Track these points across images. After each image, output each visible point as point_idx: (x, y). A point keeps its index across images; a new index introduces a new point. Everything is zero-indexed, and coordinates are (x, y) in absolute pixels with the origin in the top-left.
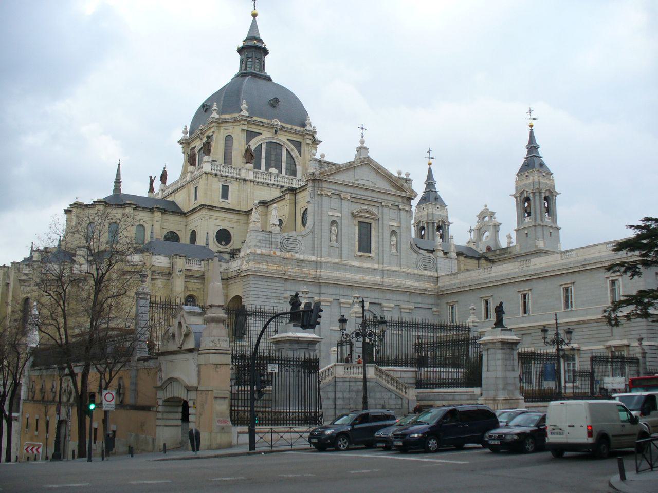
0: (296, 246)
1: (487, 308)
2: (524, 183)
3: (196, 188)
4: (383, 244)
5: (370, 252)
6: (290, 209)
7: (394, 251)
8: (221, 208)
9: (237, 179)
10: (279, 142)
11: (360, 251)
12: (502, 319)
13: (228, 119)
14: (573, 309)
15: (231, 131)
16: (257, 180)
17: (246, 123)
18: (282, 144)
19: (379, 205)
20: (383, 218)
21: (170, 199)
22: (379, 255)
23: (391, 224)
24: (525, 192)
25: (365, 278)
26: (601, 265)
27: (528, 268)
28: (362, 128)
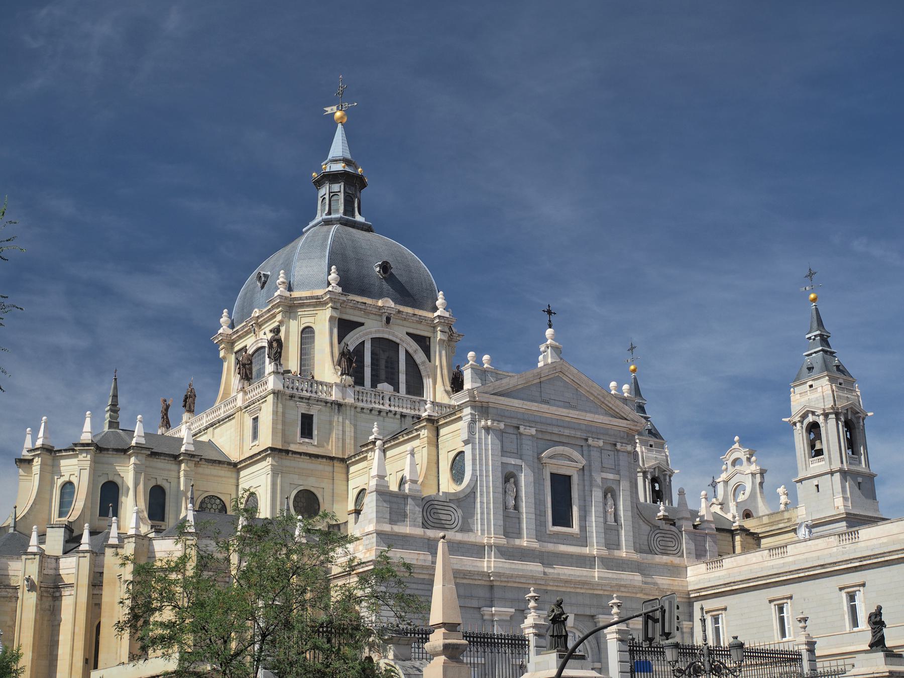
0: (449, 518)
2: (806, 398)
3: (256, 419)
8: (300, 454)
9: (326, 403)
10: (391, 338)
12: (882, 638)
13: (306, 298)
15: (311, 319)
16: (360, 404)
18: (398, 341)
19: (583, 443)
21: (204, 438)
24: (810, 415)
27: (853, 546)
28: (549, 312)
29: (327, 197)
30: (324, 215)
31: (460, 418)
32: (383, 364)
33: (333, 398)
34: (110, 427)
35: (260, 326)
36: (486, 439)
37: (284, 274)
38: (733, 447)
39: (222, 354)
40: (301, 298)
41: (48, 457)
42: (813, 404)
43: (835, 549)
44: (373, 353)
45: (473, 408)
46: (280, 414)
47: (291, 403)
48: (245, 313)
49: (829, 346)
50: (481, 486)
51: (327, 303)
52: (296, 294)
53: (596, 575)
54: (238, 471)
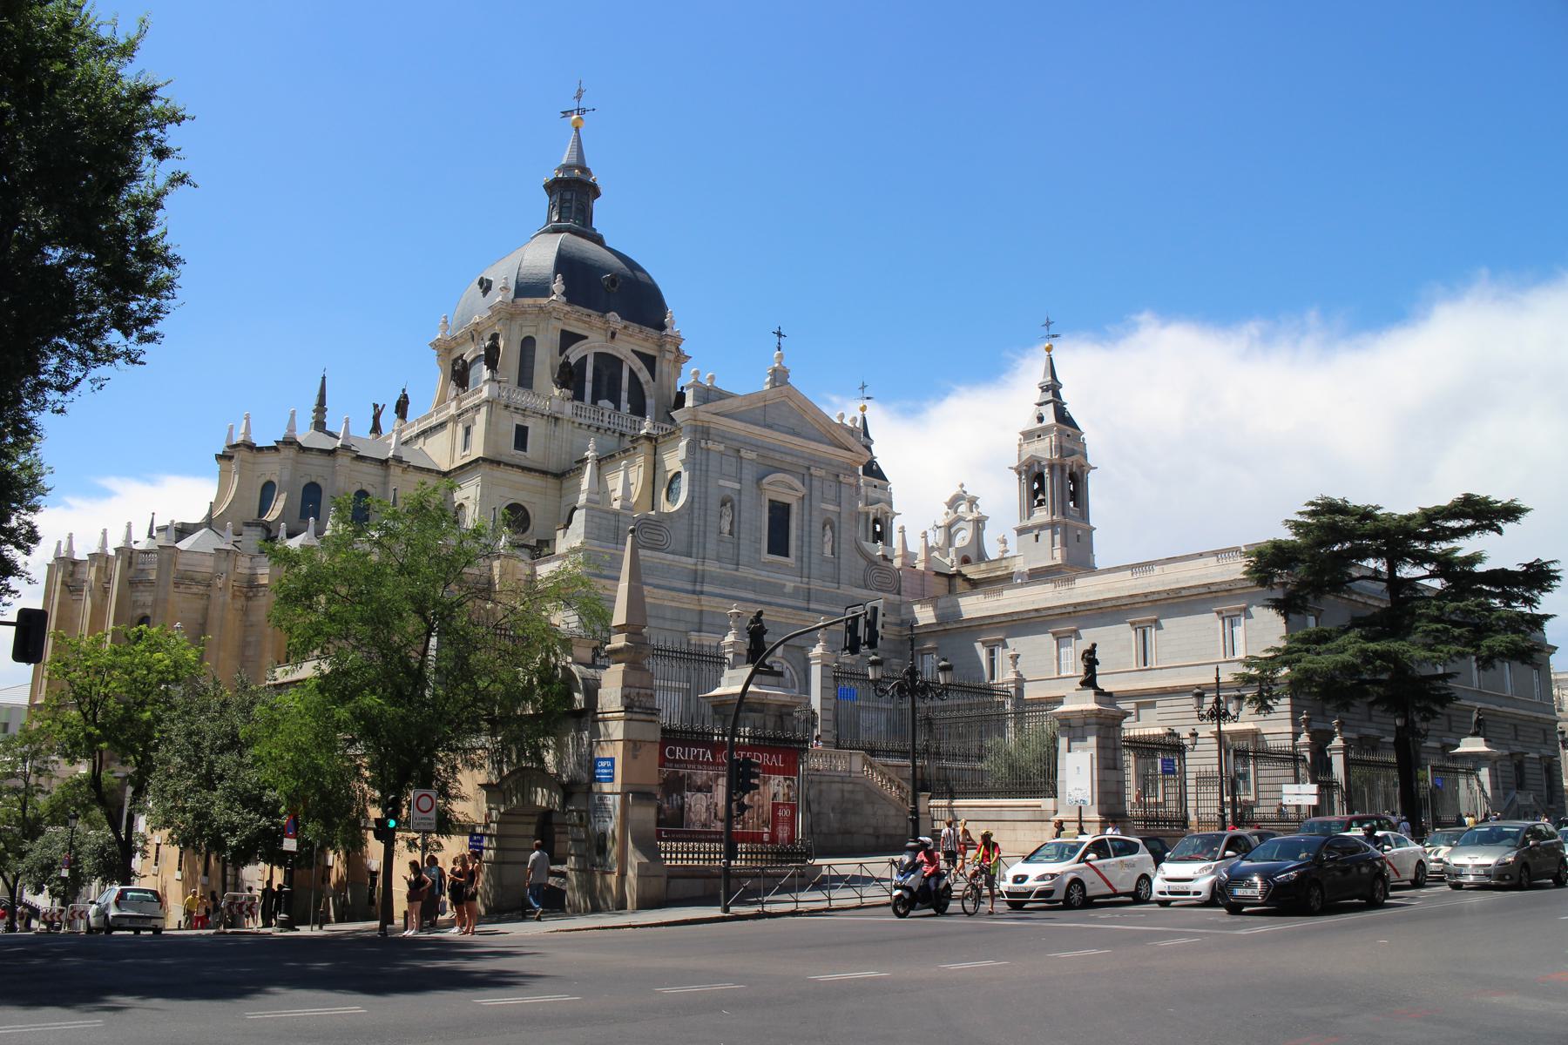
0: (661, 538)
4: (810, 542)
5: (787, 555)
7: (828, 551)
9: (543, 415)
11: (770, 552)
12: (1094, 676)
15: (533, 329)
16: (579, 420)
18: (622, 358)
19: (805, 471)
20: (811, 495)
22: (802, 561)
23: (824, 506)
26: (1208, 590)
27: (1069, 592)
32: (605, 379)
42: (1039, 454)
44: (595, 369)
47: (506, 413)
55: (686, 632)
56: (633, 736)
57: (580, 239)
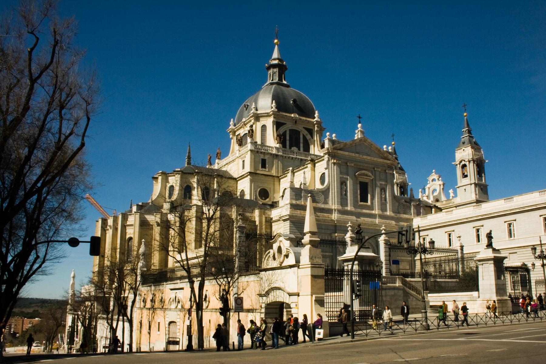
0: (319, 198)
1: (450, 239)
3: (244, 161)
6: (311, 174)
13: (263, 114)
14: (516, 238)
15: (265, 122)
16: (285, 155)
17: (276, 116)
18: (300, 130)
19: (373, 170)
24: (463, 161)
25: (365, 220)
28: (360, 117)
29: (272, 74)
30: (270, 81)
31: (323, 160)
33: (274, 152)
34: (187, 165)
35: (245, 125)
36: (334, 167)
37: (255, 104)
38: (432, 174)
39: (231, 136)
40: (261, 114)
41: (164, 176)
42: (464, 157)
43: (472, 212)
45: (329, 155)
46: (253, 159)
47: (257, 155)
48: (240, 120)
49: (471, 134)
50: (332, 186)
51: (271, 116)
52: (259, 112)
53: (377, 221)
54: (237, 181)
55: (331, 234)
56: (314, 274)
57: (281, 86)
